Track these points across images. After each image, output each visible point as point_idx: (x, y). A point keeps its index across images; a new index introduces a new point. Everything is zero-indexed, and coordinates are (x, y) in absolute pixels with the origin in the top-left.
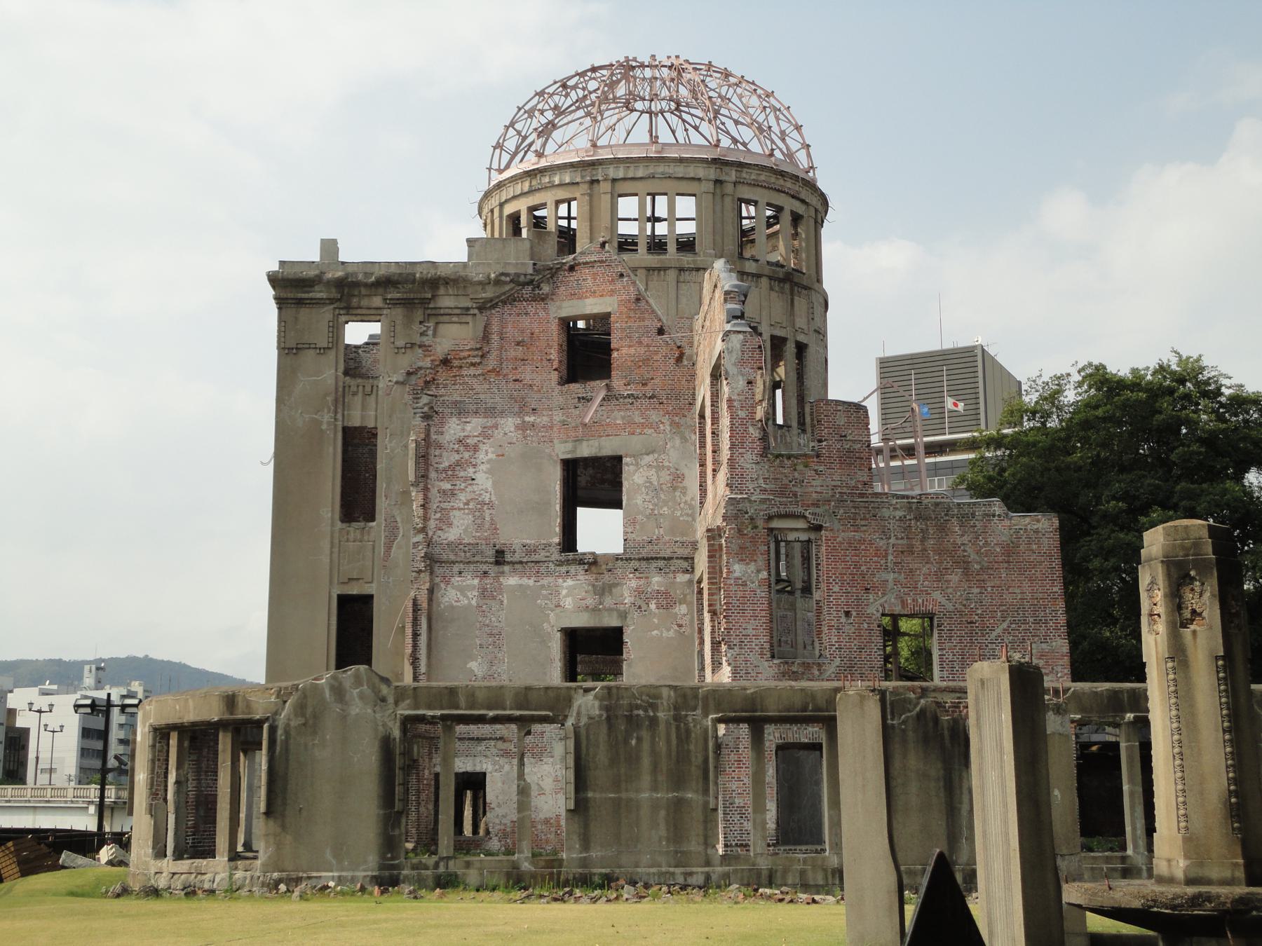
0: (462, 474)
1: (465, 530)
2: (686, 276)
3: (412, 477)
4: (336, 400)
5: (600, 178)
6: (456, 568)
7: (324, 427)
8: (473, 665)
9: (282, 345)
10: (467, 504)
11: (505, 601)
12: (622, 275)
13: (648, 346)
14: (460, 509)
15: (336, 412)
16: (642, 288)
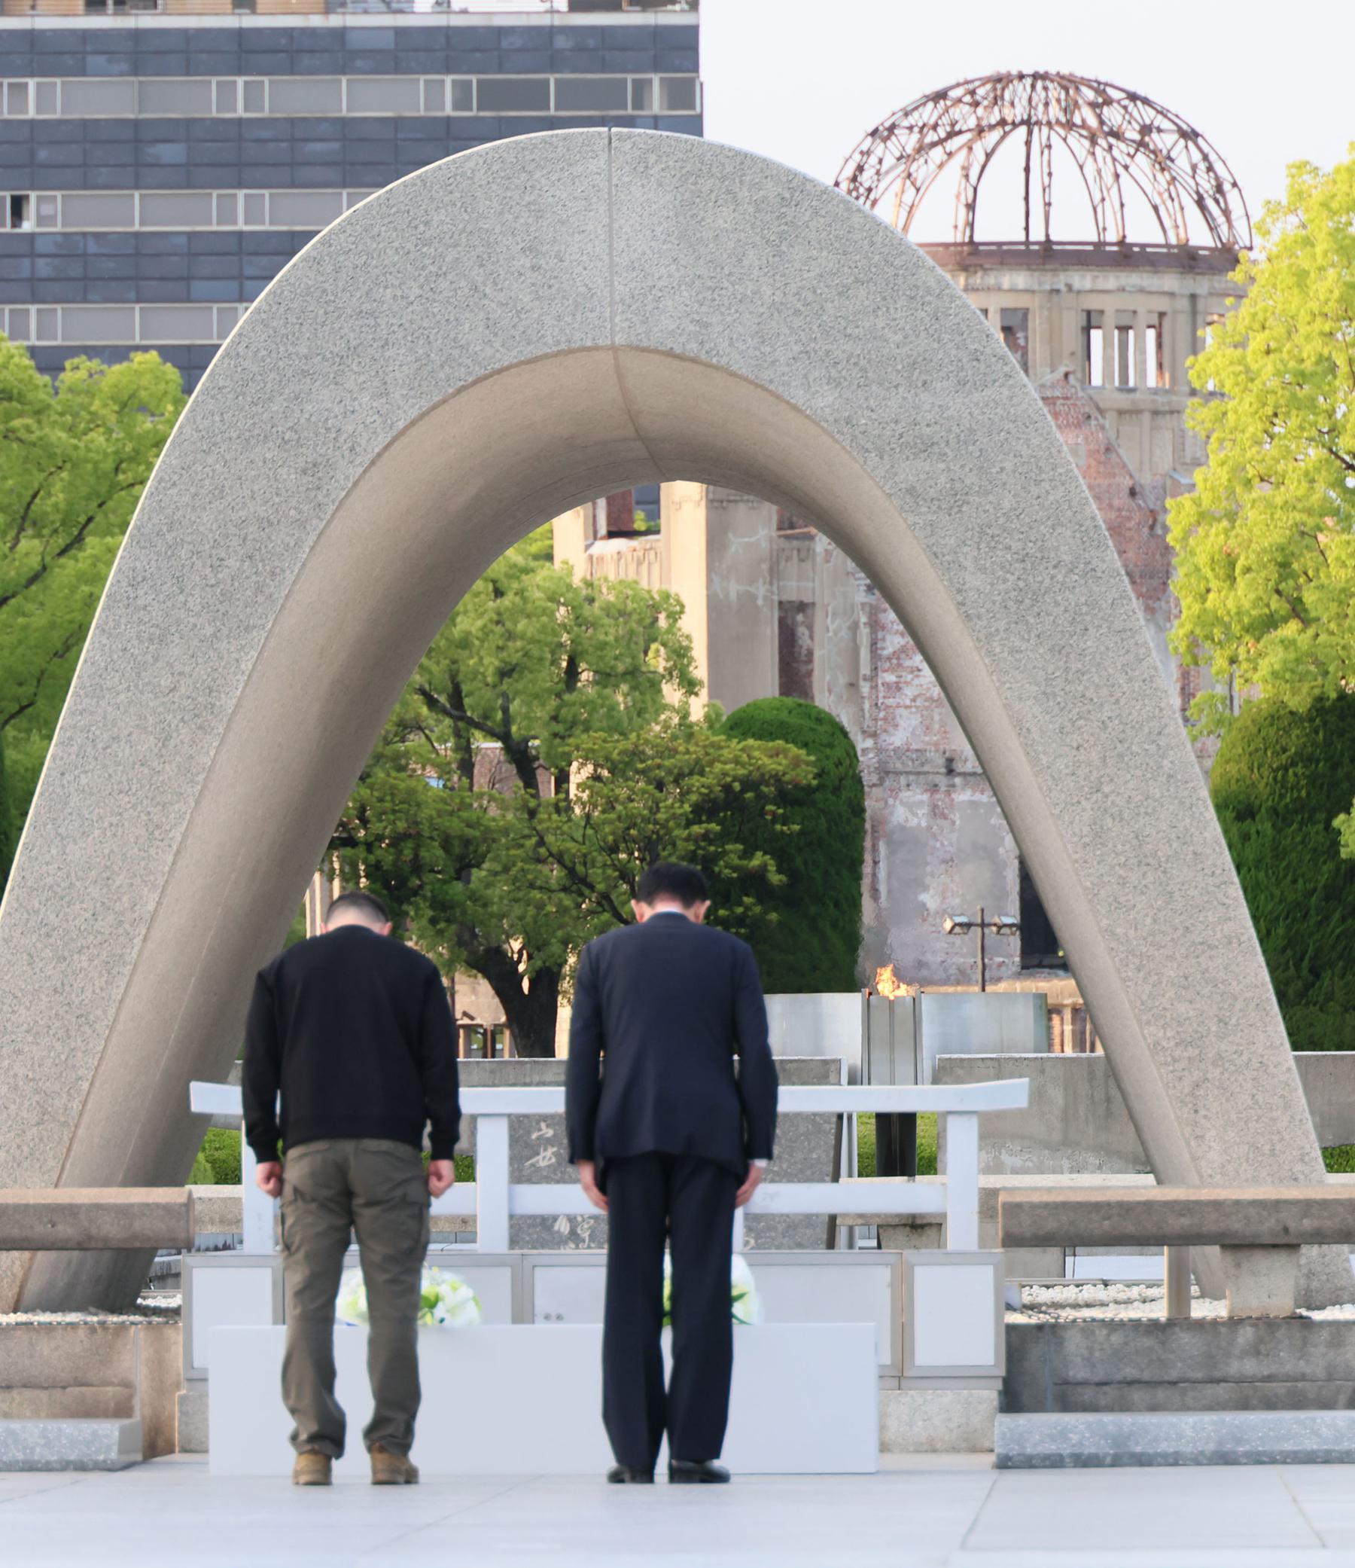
0: (907, 663)
1: (913, 733)
2: (1161, 421)
3: (865, 669)
4: (771, 570)
5: (1062, 287)
6: (903, 780)
7: (760, 602)
8: (924, 897)
9: (711, 496)
10: (914, 700)
11: (958, 822)
12: (1089, 417)
13: (1119, 510)
14: (906, 707)
15: (771, 584)
16: (1112, 435)
